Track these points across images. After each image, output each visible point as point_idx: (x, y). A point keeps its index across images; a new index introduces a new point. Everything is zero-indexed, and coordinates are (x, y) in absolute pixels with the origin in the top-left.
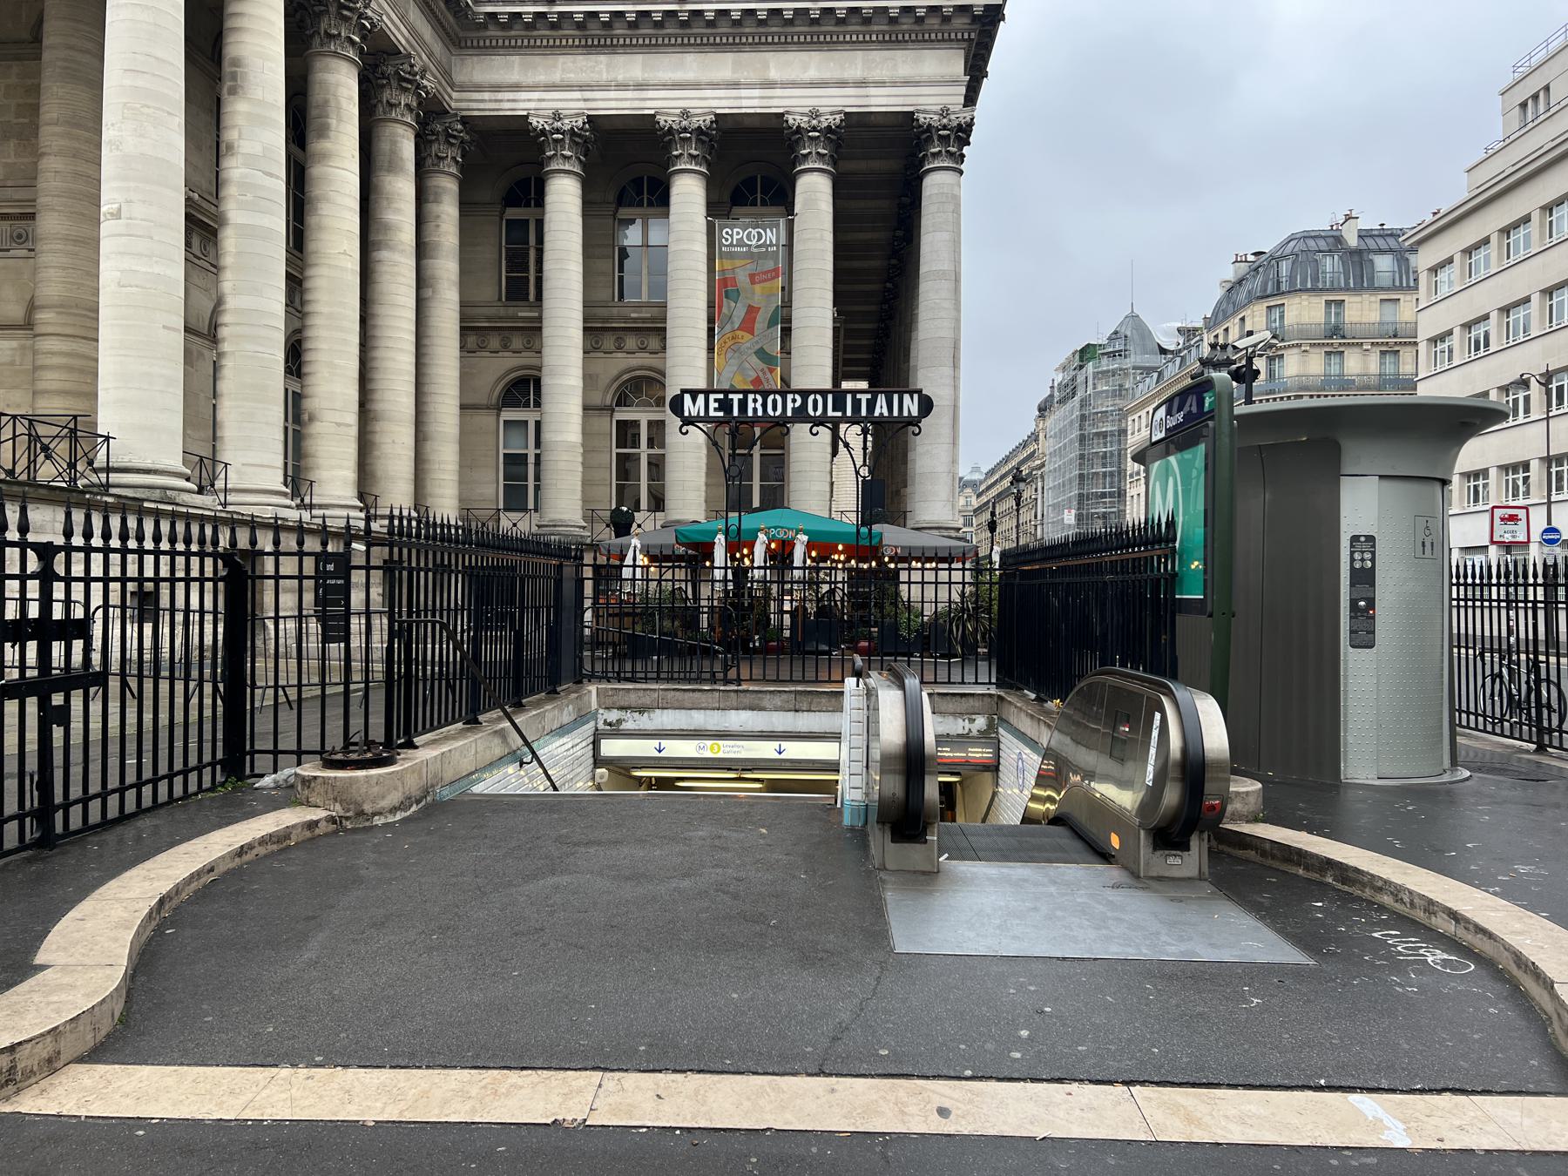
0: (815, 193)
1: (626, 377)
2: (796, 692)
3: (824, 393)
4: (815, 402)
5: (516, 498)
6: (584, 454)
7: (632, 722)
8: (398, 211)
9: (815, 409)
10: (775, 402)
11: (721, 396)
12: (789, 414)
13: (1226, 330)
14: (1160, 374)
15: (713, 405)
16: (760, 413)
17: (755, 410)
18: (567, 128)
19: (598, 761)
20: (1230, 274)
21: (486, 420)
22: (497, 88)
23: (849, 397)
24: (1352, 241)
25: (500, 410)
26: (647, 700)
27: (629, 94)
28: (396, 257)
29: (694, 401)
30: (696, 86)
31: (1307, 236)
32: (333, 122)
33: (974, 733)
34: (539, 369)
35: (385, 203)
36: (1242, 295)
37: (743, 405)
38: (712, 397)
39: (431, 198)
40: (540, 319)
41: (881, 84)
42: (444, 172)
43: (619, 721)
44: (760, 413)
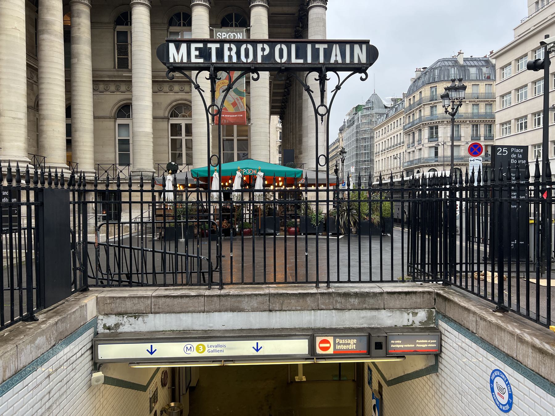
1: (174, 104)
2: (270, 295)
4: (281, 51)
5: (125, 159)
6: (154, 138)
7: (129, 325)
8: (53, 15)
9: (281, 56)
10: (247, 50)
11: (201, 45)
12: (259, 60)
13: (414, 97)
14: (387, 115)
15: (194, 53)
16: (235, 60)
17: (230, 57)
19: (97, 365)
20: (414, 76)
21: (109, 124)
23: (309, 47)
24: (461, 62)
26: (141, 306)
28: (52, 38)
29: (178, 49)
31: (444, 60)
33: (417, 324)
34: (131, 99)
35: (45, 11)
36: (420, 83)
37: (220, 53)
38: (193, 46)
39: (76, 15)
40: (131, 77)
42: (82, 3)
43: (117, 325)
44: (235, 60)
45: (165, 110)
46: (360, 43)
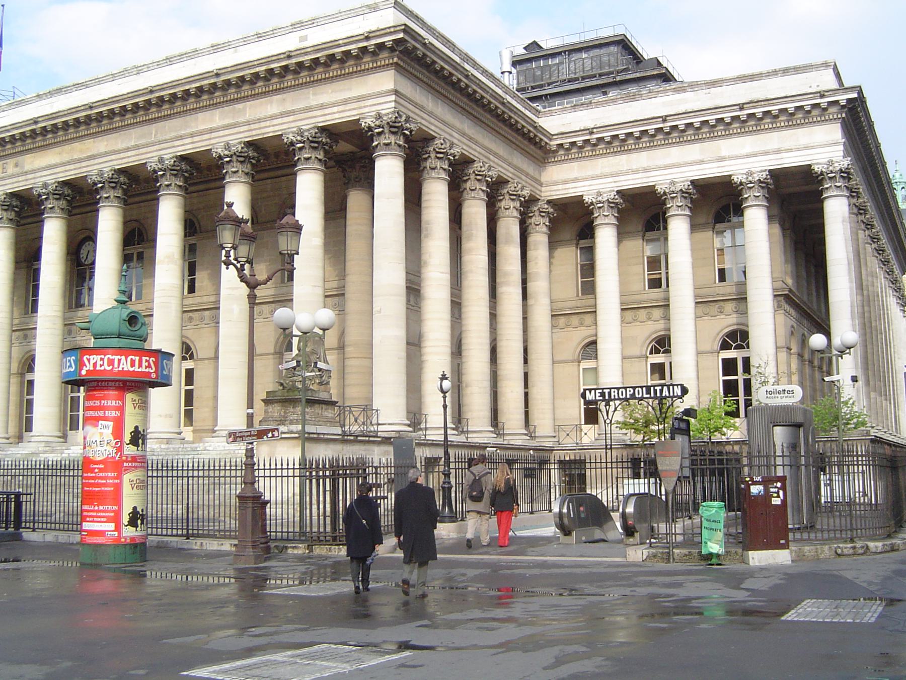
0: (756, 218)
3: (642, 387)
15: (598, 395)
18: (605, 199)
21: (570, 368)
22: (566, 182)
25: (580, 362)
27: (640, 175)
30: (678, 166)
32: (474, 232)
37: (610, 393)
39: (532, 248)
41: (790, 150)
45: (642, 346)
46: (677, 385)
